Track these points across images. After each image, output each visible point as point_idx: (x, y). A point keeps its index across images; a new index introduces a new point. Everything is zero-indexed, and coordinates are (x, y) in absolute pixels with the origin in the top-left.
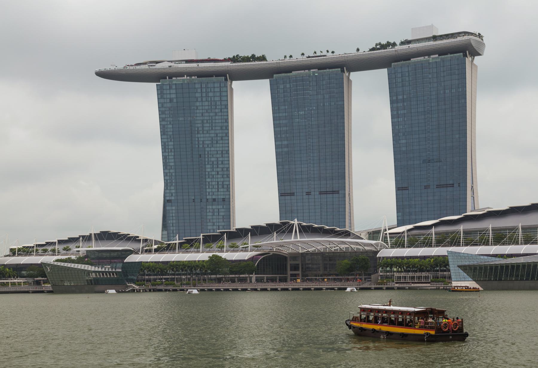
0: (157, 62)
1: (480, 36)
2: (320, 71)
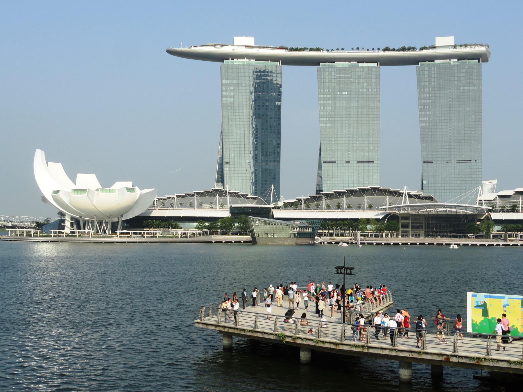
0: (223, 46)
2: (361, 64)
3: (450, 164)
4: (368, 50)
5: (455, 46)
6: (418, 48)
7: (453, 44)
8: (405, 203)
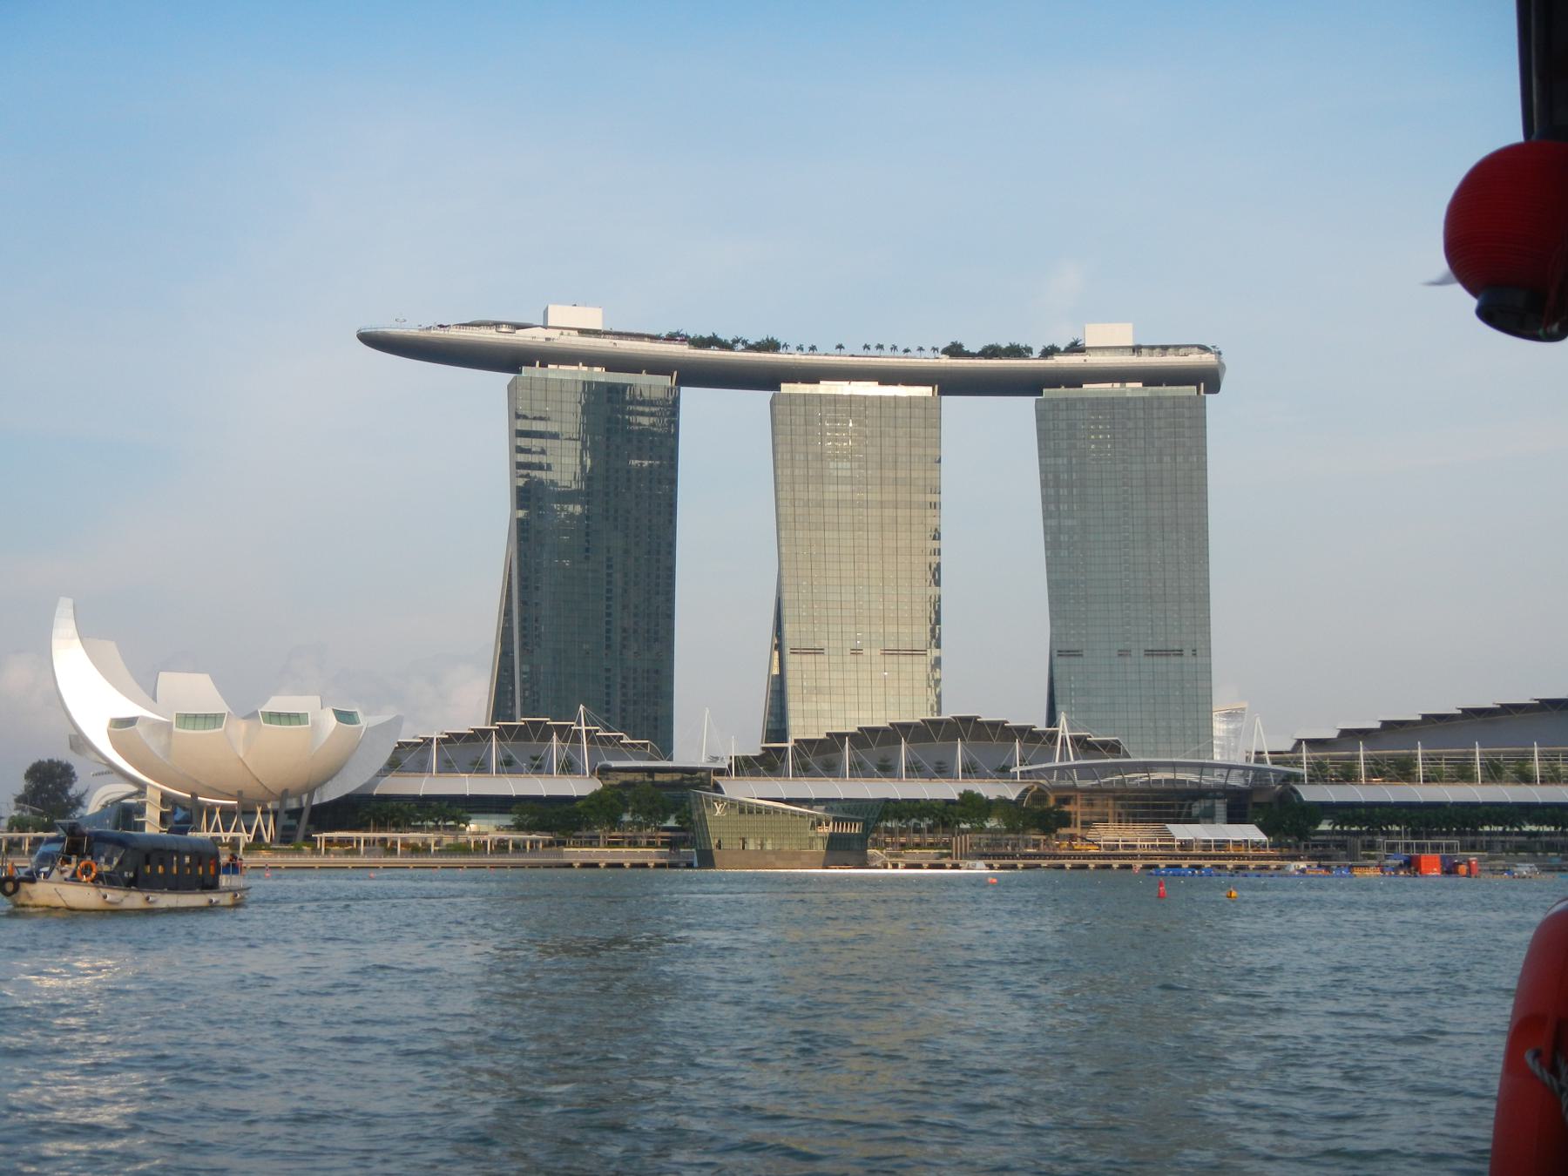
3: (1128, 660)
4: (906, 351)
6: (1036, 353)
7: (1131, 344)
8: (1061, 759)
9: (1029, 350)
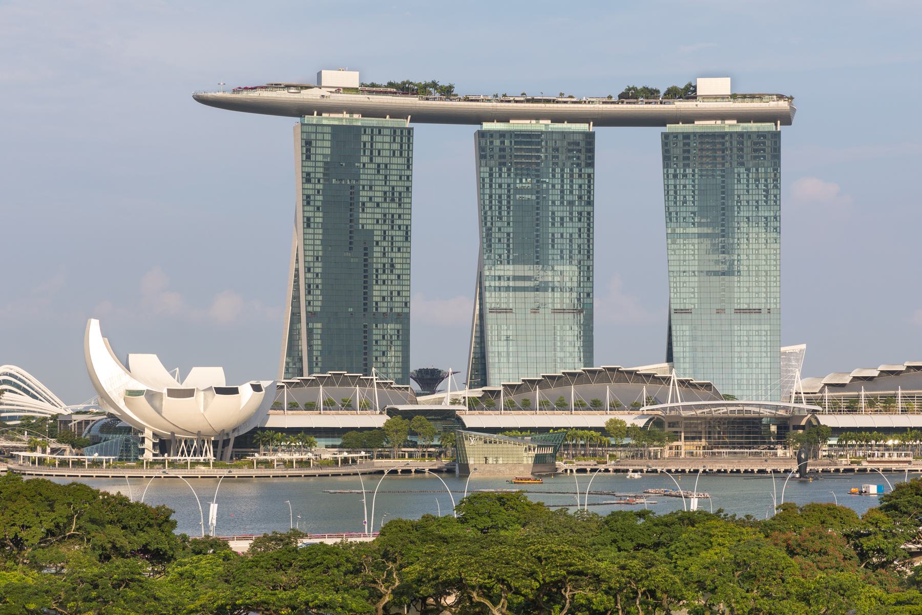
1: (792, 98)
3: (723, 316)
5: (734, 97)
6: (662, 94)
9: (658, 92)
